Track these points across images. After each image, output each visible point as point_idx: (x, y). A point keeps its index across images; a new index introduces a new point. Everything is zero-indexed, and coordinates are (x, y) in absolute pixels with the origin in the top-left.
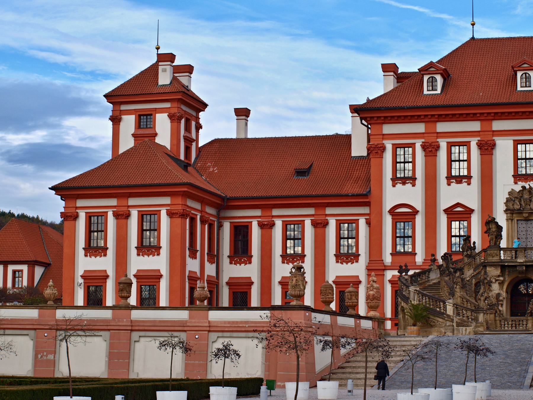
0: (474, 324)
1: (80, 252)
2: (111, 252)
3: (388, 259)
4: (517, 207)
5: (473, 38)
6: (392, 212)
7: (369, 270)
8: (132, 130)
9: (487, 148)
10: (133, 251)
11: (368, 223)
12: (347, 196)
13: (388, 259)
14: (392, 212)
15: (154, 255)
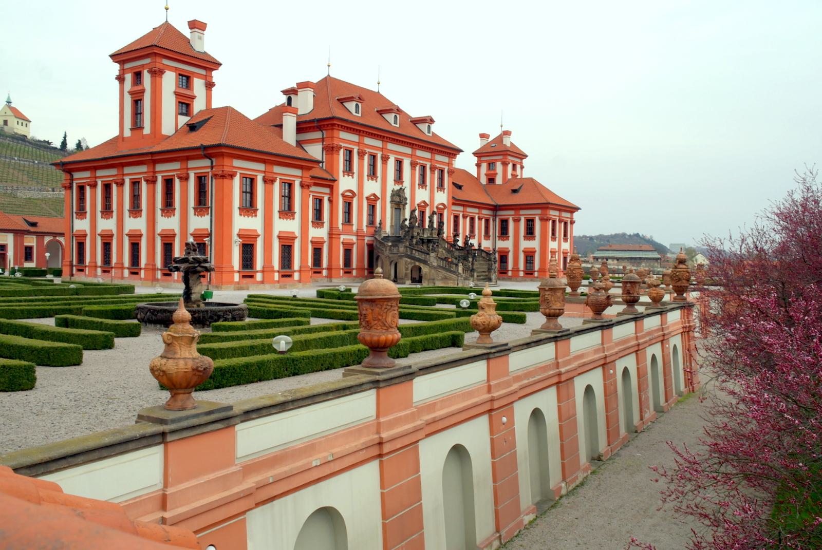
0: (472, 279)
1: (236, 212)
2: (260, 213)
3: (340, 227)
4: (397, 199)
5: (329, 75)
6: (343, 195)
7: (330, 235)
8: (173, 88)
9: (385, 159)
10: (276, 215)
11: (330, 201)
12: (326, 180)
13: (340, 227)
14: (343, 195)
15: (252, 216)
